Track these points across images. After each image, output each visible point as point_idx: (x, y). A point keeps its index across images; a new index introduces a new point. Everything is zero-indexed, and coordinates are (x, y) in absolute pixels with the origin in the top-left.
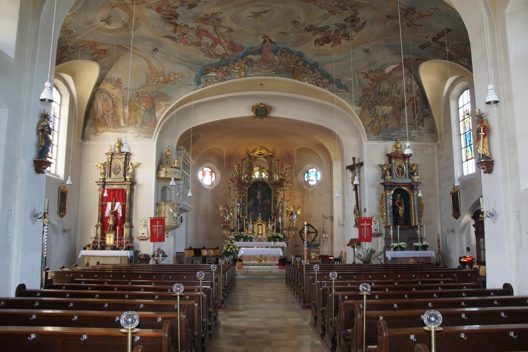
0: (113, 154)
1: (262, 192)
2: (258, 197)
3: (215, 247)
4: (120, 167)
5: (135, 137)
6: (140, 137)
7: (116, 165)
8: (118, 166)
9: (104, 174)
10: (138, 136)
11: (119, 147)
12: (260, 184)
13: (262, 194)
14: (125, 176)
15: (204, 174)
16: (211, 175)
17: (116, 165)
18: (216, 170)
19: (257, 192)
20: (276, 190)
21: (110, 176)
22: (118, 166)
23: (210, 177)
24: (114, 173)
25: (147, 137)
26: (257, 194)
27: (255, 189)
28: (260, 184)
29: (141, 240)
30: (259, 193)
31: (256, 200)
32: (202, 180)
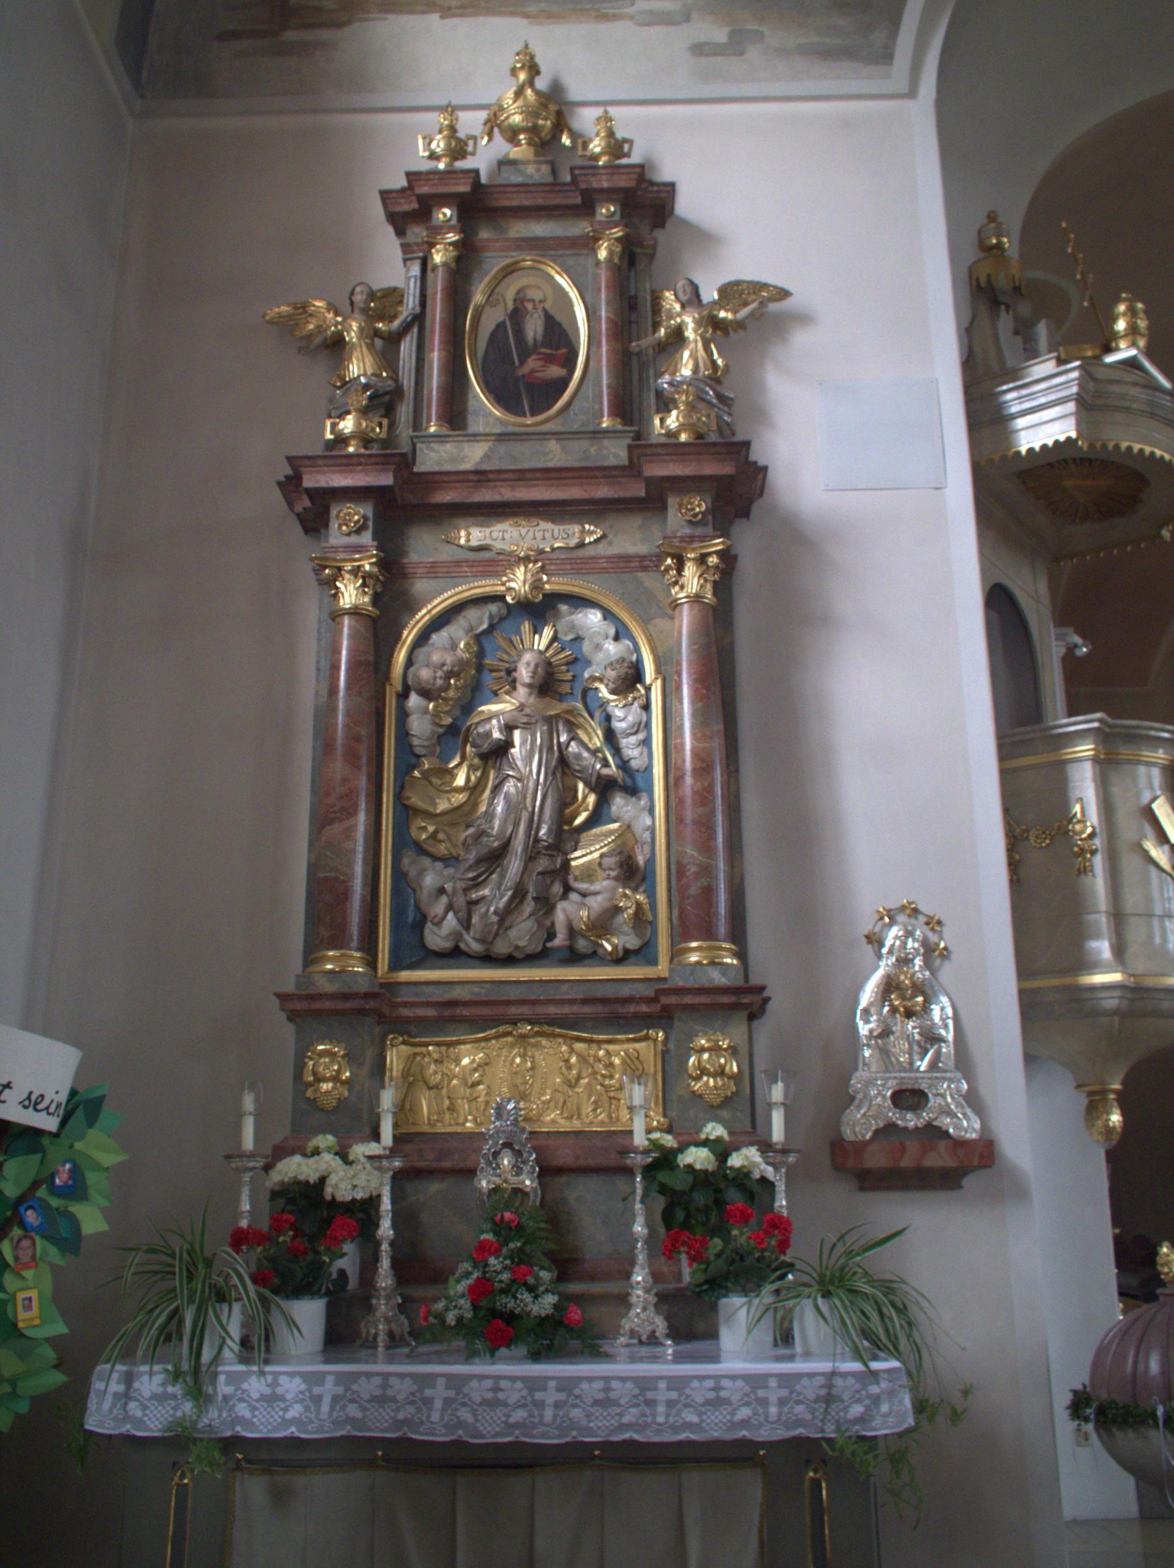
0: (478, 204)
4: (558, 337)
5: (699, 49)
6: (753, 53)
7: (517, 315)
8: (534, 328)
9: (383, 402)
10: (736, 45)
11: (545, 144)
14: (628, 406)
17: (517, 315)
21: (455, 414)
22: (534, 328)
24: (504, 396)
25: (827, 54)
29: (872, 1180)
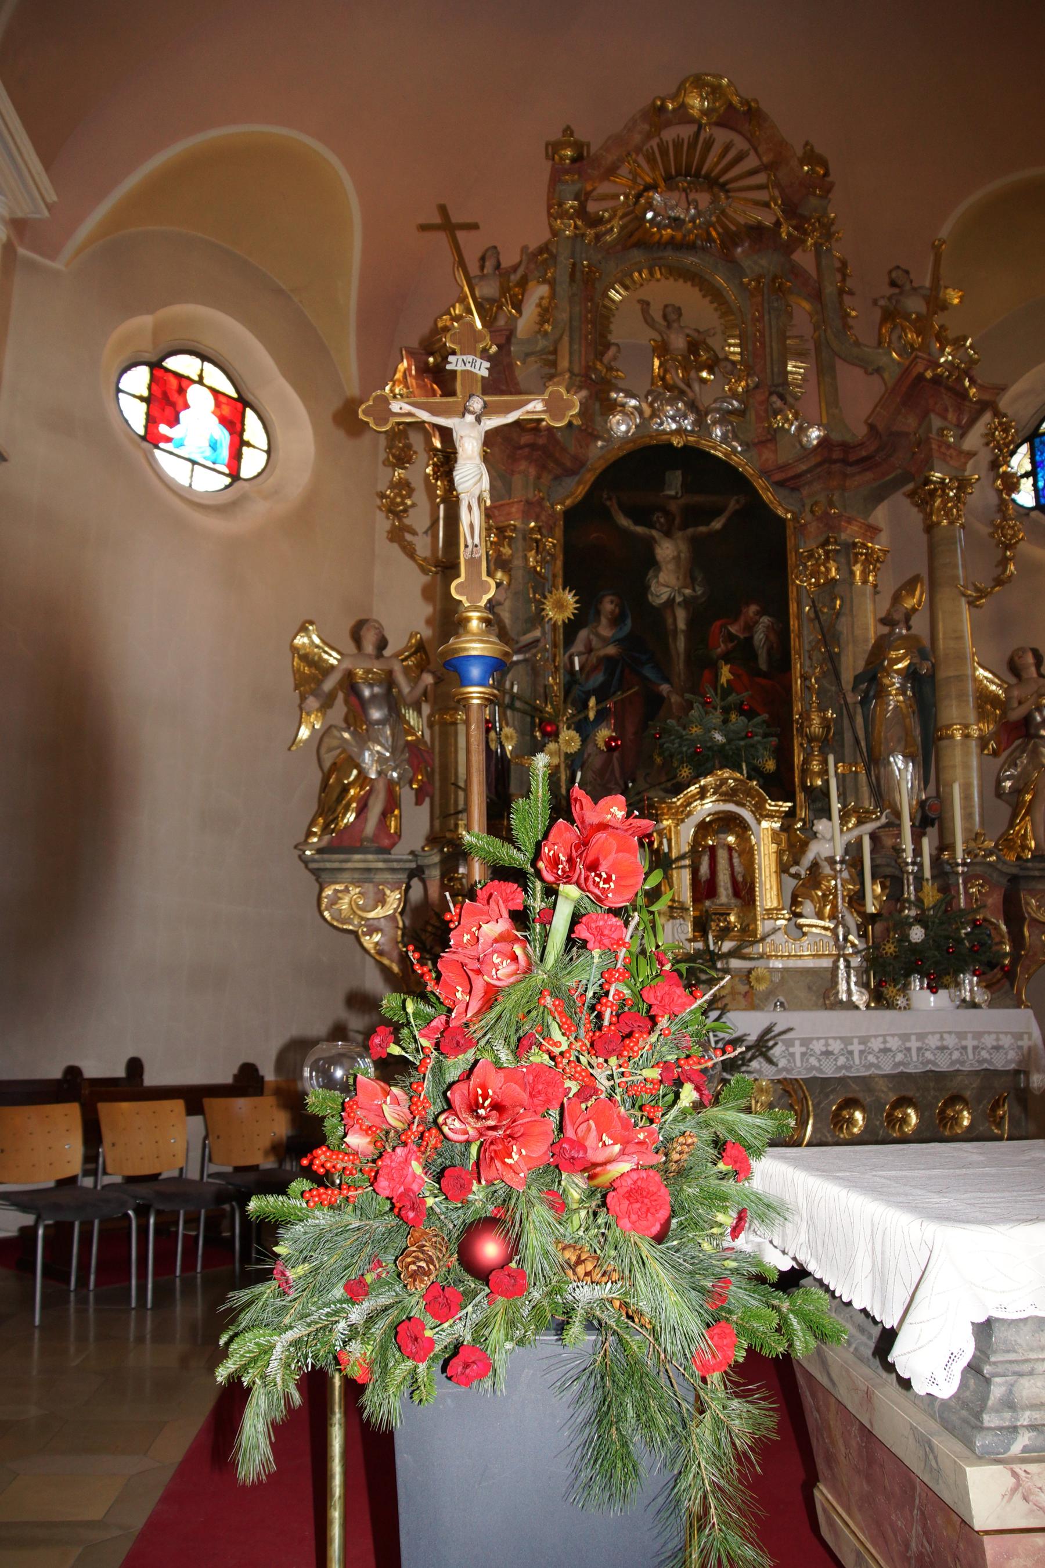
1: (695, 542)
2: (666, 585)
3: (225, 1076)
12: (674, 483)
13: (701, 559)
15: (166, 400)
16: (234, 425)
18: (277, 388)
19: (648, 547)
20: (830, 524)
23: (223, 436)
26: (651, 563)
27: (641, 516)
28: (674, 483)
30: (666, 550)
31: (645, 625)
32: (152, 438)
